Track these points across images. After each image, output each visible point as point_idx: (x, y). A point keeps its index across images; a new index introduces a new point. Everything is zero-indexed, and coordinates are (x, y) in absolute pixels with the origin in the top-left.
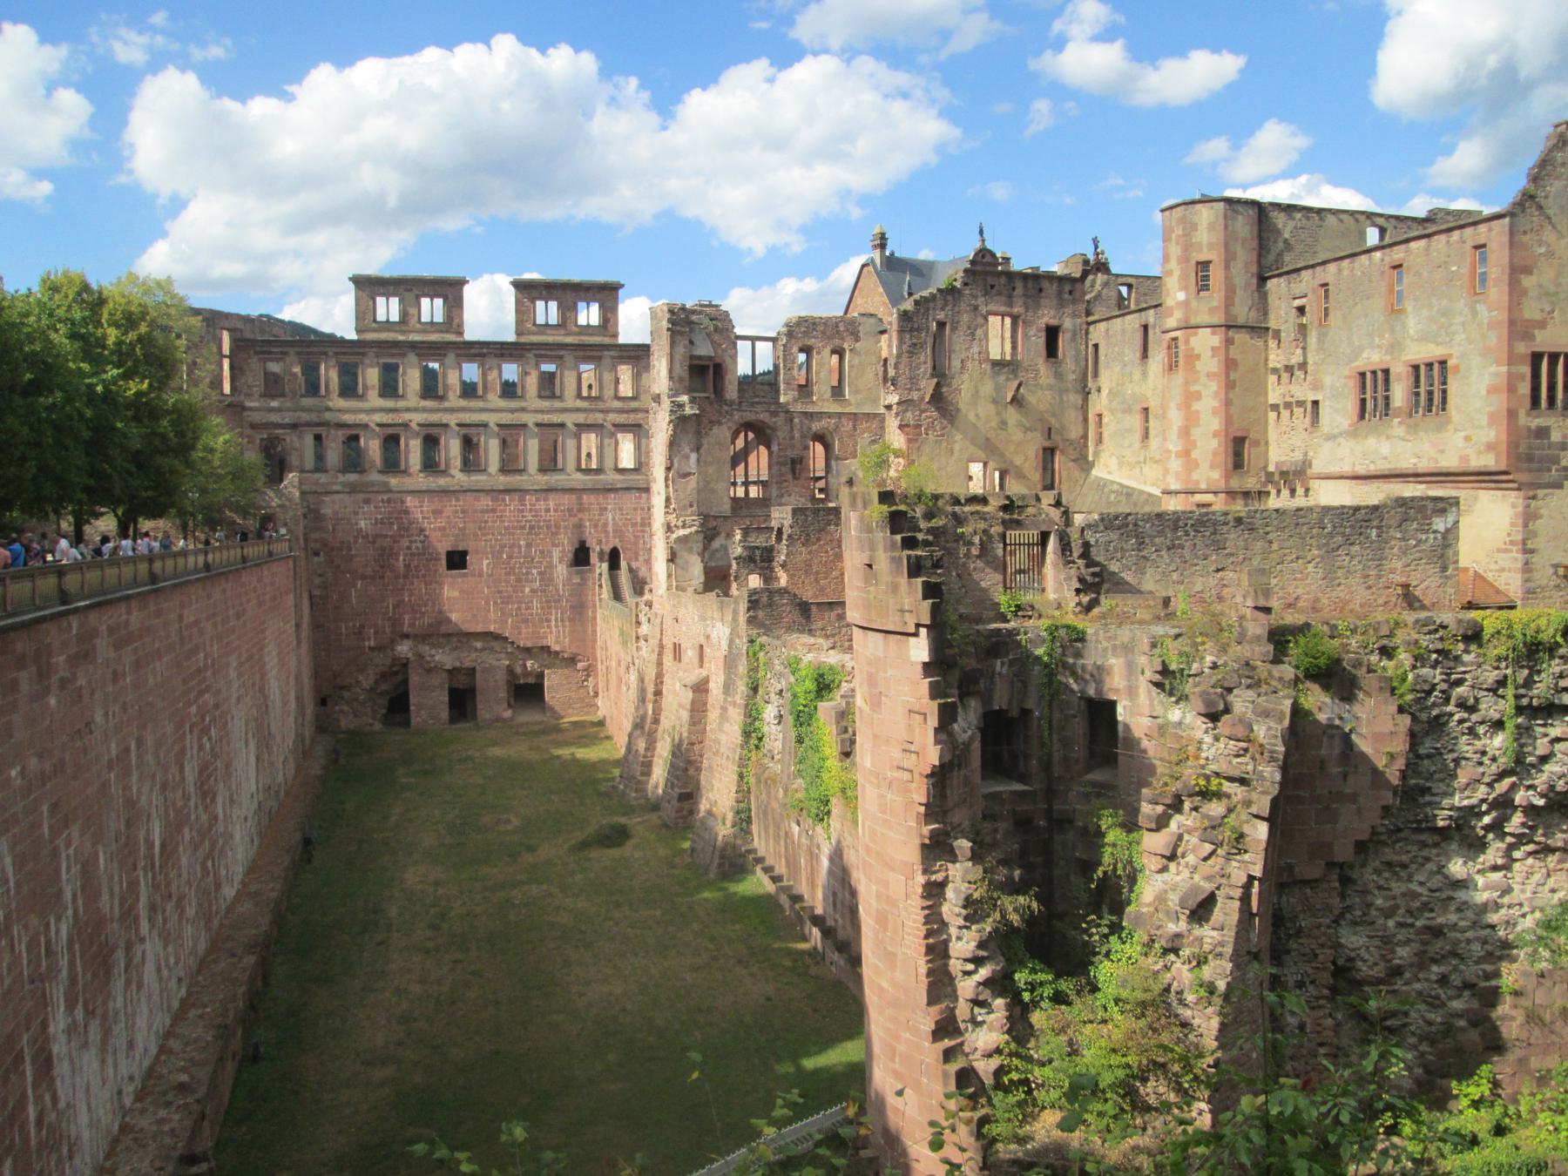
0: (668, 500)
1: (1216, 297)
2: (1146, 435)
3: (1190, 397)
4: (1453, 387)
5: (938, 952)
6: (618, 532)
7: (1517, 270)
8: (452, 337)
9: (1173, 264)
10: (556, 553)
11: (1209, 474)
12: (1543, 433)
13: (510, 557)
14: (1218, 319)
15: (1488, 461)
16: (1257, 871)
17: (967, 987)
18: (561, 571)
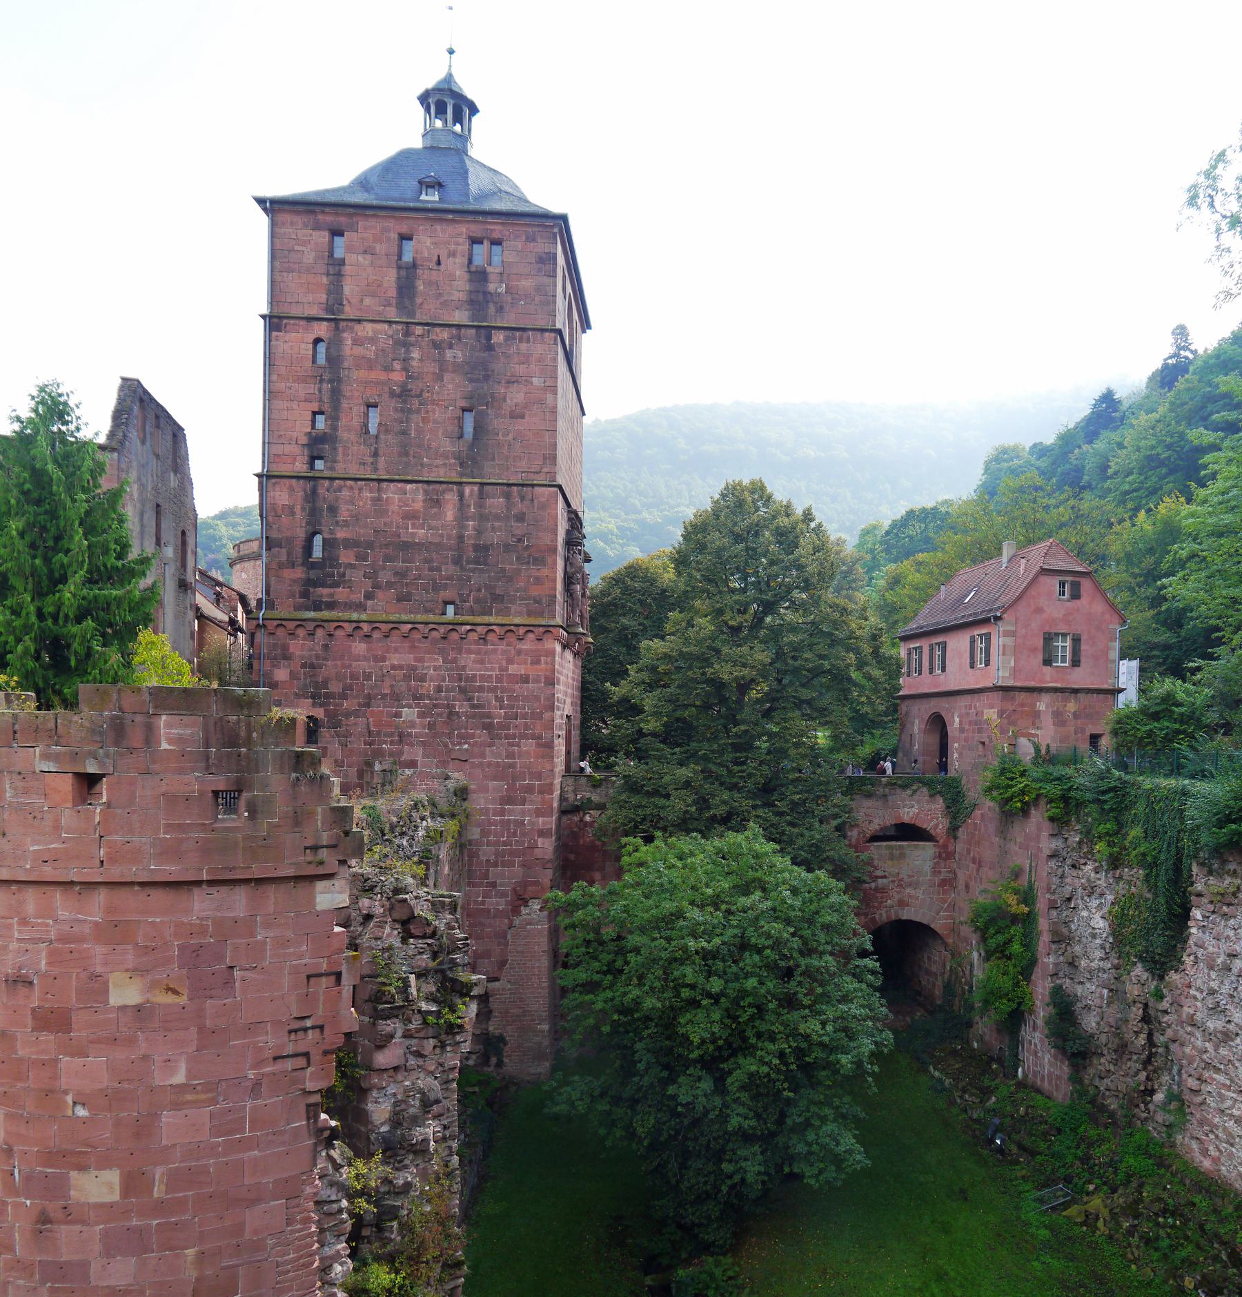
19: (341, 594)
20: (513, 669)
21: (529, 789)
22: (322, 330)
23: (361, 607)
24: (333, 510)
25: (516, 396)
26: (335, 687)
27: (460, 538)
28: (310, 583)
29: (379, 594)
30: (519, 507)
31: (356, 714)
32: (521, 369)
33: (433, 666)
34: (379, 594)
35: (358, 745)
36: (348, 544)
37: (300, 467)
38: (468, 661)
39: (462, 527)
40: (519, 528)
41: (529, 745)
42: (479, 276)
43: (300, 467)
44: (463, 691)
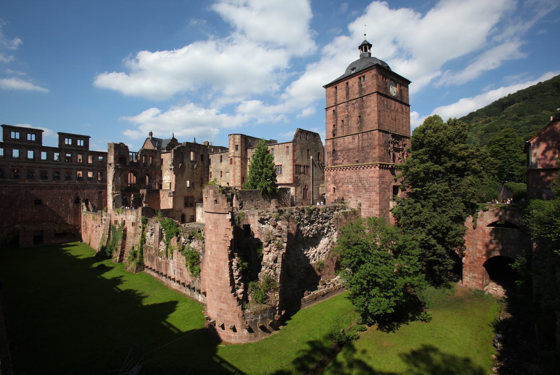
0: (113, 188)
1: (239, 152)
2: (221, 176)
3: (235, 170)
4: (283, 170)
5: (231, 276)
6: (88, 195)
7: (294, 151)
8: (38, 145)
9: (231, 145)
10: (70, 201)
11: (238, 184)
12: (297, 177)
13: (55, 201)
14: (240, 155)
15: (290, 182)
16: (284, 252)
17: (236, 281)
18: (71, 205)
19: (338, 162)
20: (370, 175)
21: (374, 204)
22: (334, 108)
23: (341, 164)
24: (337, 144)
25: (368, 110)
26: (338, 181)
27: (359, 146)
28: (333, 160)
29: (345, 161)
30: (370, 136)
31: (341, 187)
32: (369, 104)
33: (354, 175)
34: (345, 161)
35: (341, 193)
36: (339, 151)
37: (331, 137)
38: (361, 174)
39: (359, 143)
40: (370, 141)
41: (374, 193)
42: (360, 86)
43: (331, 137)
44: (360, 181)
